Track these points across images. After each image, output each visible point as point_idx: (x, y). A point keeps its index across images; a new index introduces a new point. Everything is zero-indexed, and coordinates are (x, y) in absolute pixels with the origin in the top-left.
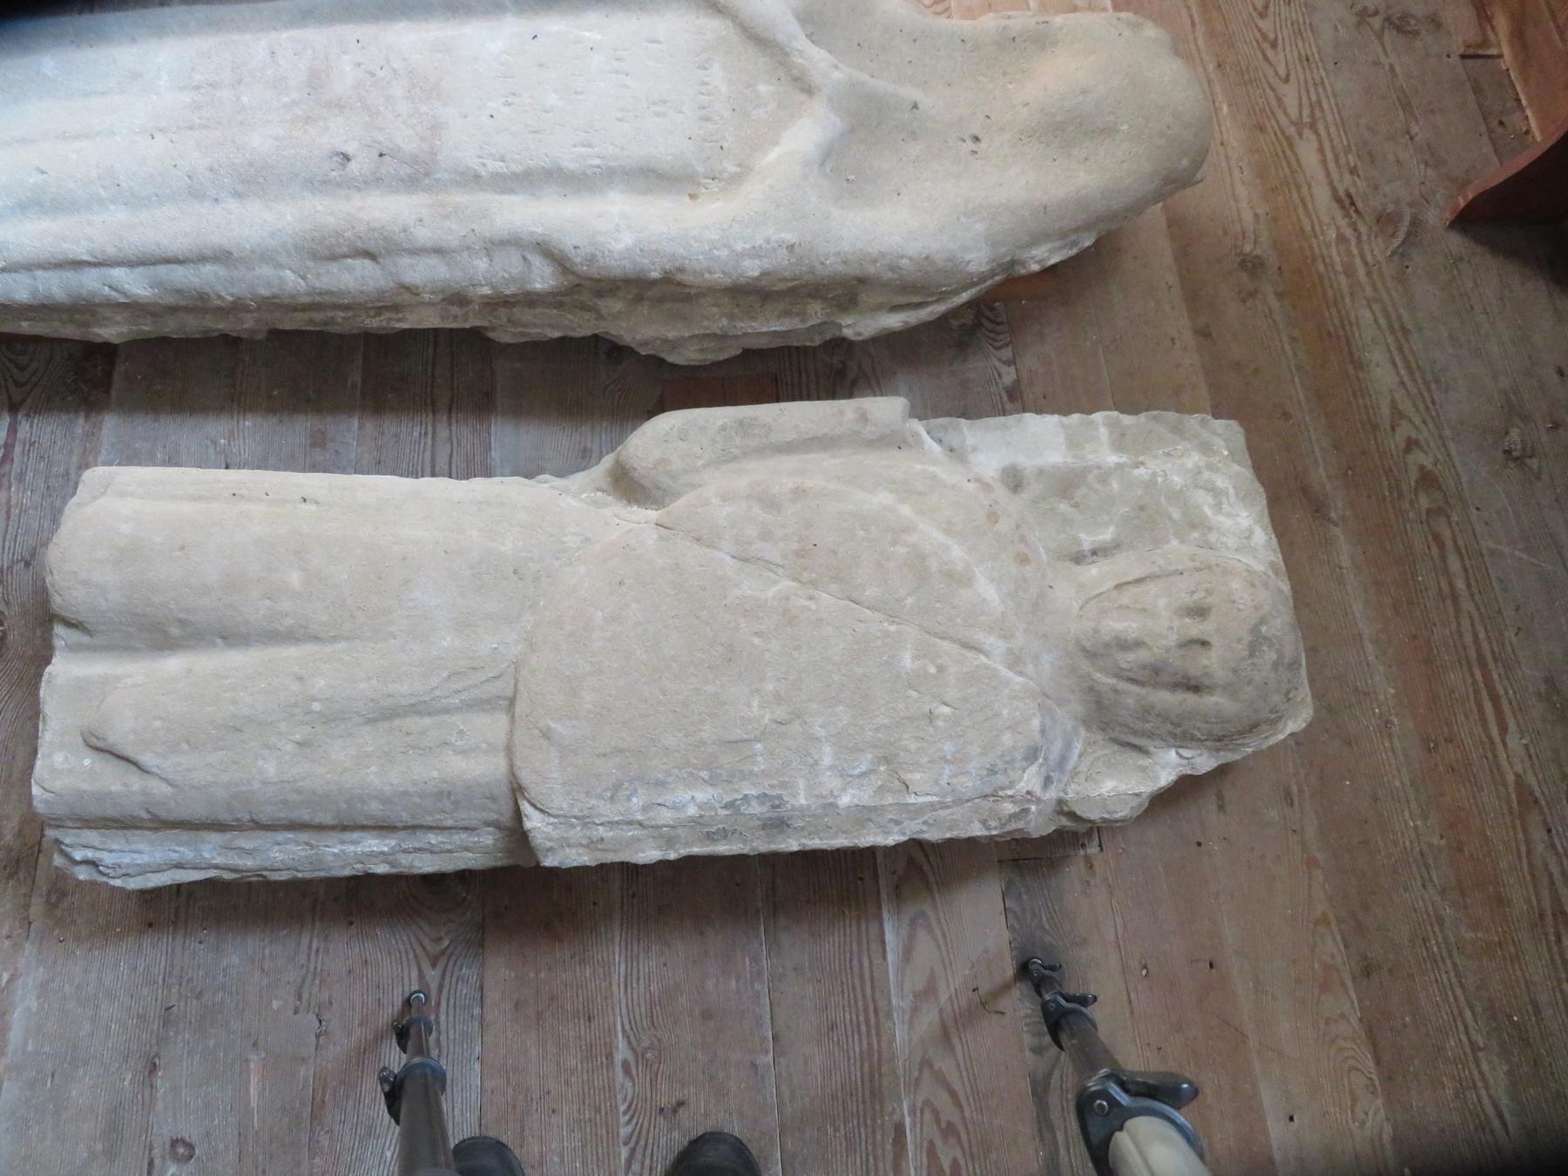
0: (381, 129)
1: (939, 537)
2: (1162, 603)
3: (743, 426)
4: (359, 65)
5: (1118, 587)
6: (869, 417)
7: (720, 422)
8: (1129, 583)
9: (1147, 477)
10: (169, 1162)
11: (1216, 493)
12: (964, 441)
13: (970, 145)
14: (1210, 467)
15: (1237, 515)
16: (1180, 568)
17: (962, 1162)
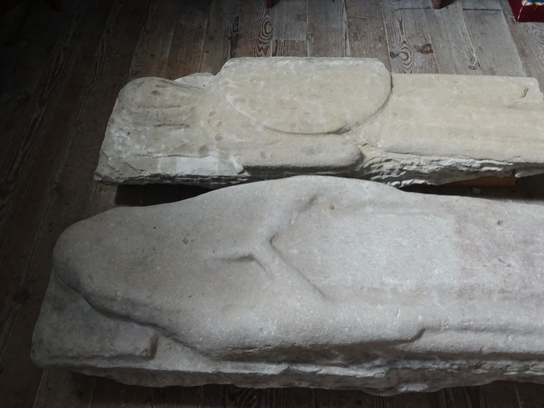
0: (486, 233)
1: (244, 112)
2: (167, 98)
3: (311, 152)
4: (509, 266)
5: (179, 106)
6: (261, 154)
7: (322, 155)
8: (175, 106)
9: (149, 148)
10: (475, 66)
11: (123, 144)
12: (219, 166)
13: (189, 239)
14: (120, 152)
15: (118, 137)
16: (155, 110)
17: (258, 51)
